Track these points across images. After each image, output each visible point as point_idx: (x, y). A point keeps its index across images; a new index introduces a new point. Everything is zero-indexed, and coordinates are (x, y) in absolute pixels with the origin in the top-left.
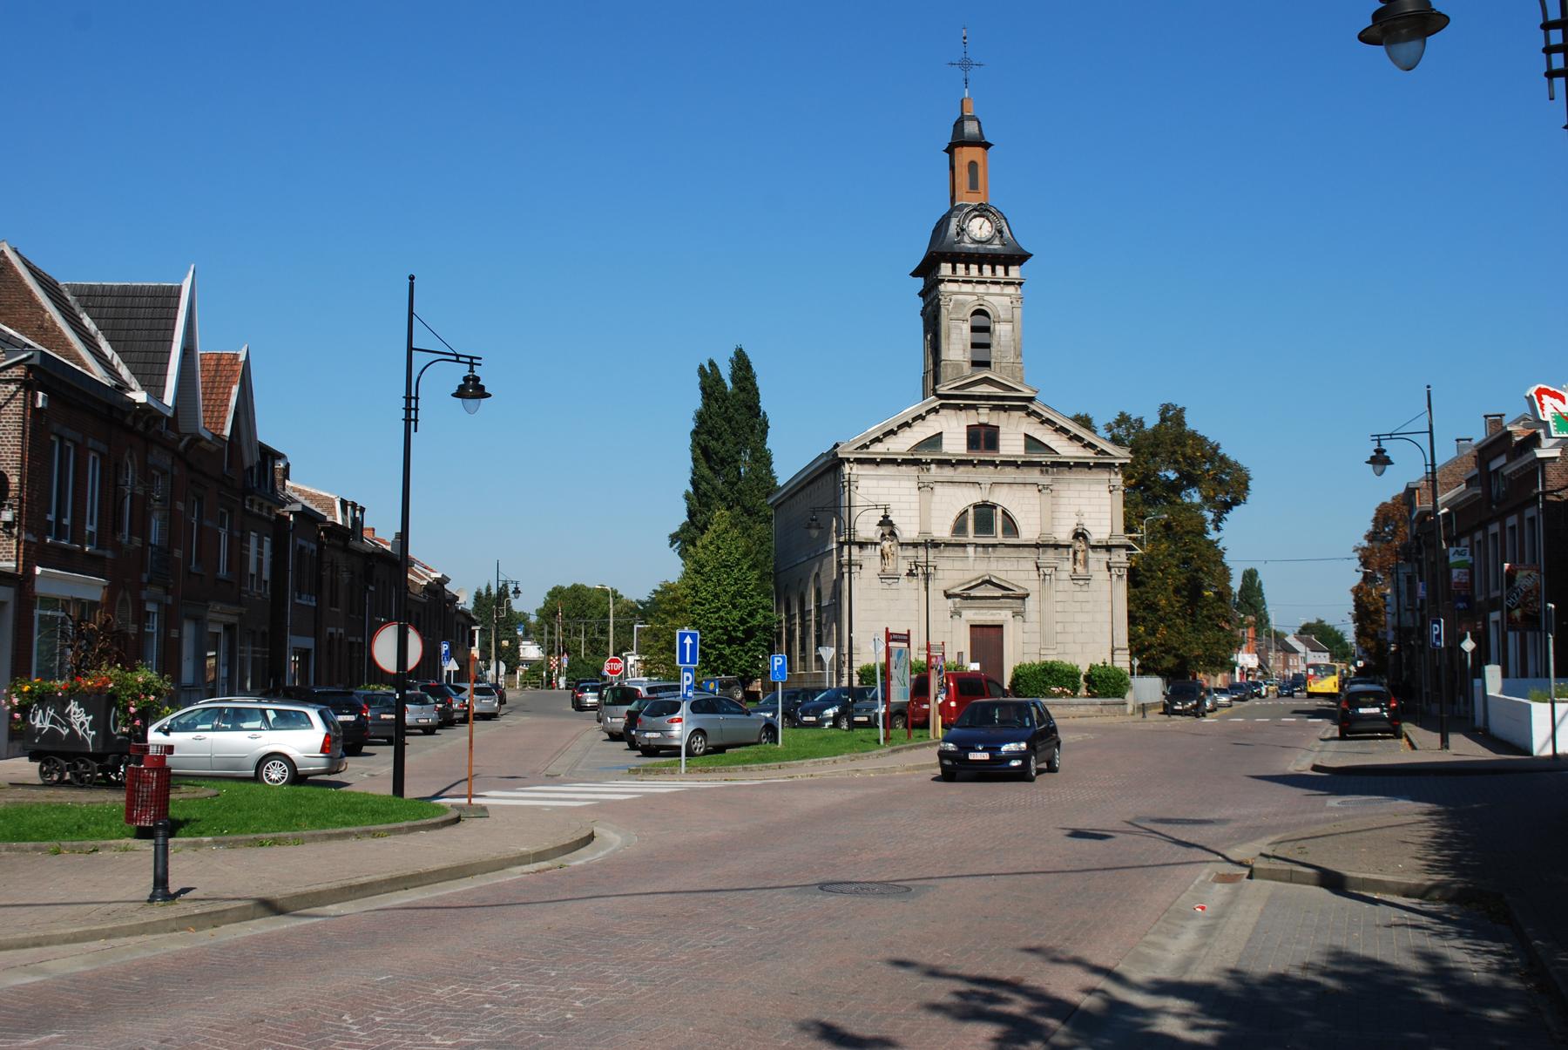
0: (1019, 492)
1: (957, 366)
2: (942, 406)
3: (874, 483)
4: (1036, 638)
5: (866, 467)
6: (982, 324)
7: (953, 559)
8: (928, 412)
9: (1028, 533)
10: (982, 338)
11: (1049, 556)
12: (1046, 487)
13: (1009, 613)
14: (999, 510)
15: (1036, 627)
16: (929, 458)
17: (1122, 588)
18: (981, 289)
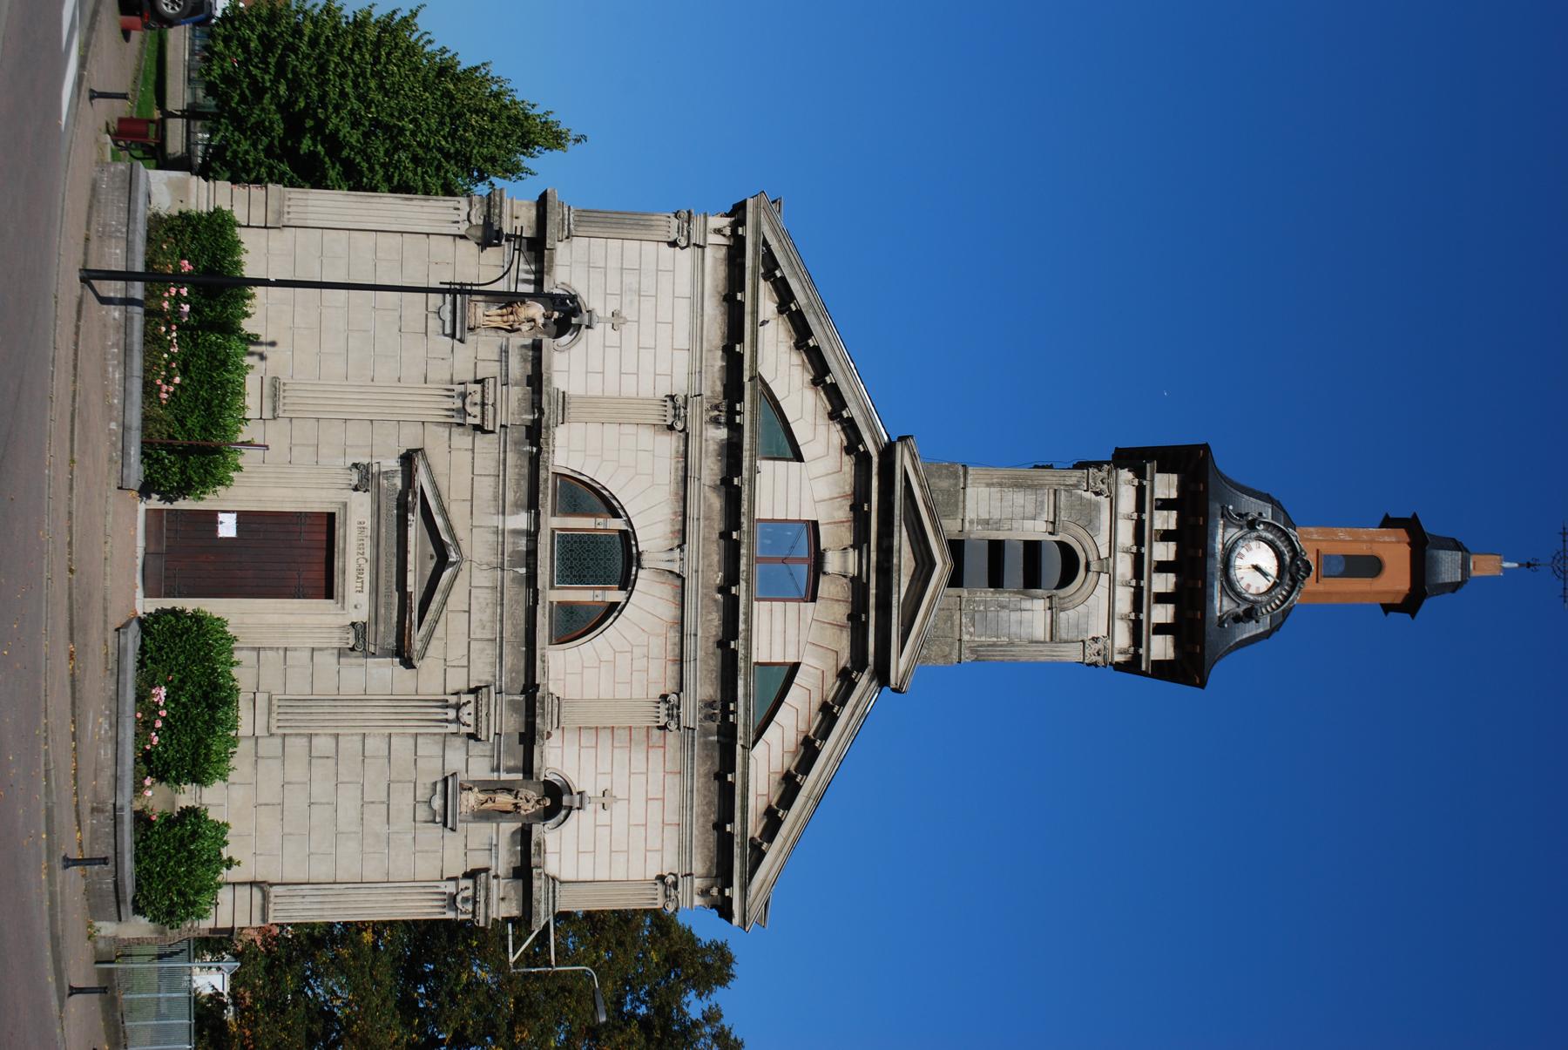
0: (661, 645)
1: (955, 501)
2: (862, 461)
3: (684, 286)
4: (298, 686)
5: (722, 271)
6: (1045, 567)
7: (500, 476)
8: (850, 427)
9: (567, 669)
10: (1014, 566)
11: (504, 720)
12: (674, 712)
13: (362, 615)
14: (616, 596)
15: (325, 686)
16: (746, 420)
17: (421, 907)
18: (1124, 566)
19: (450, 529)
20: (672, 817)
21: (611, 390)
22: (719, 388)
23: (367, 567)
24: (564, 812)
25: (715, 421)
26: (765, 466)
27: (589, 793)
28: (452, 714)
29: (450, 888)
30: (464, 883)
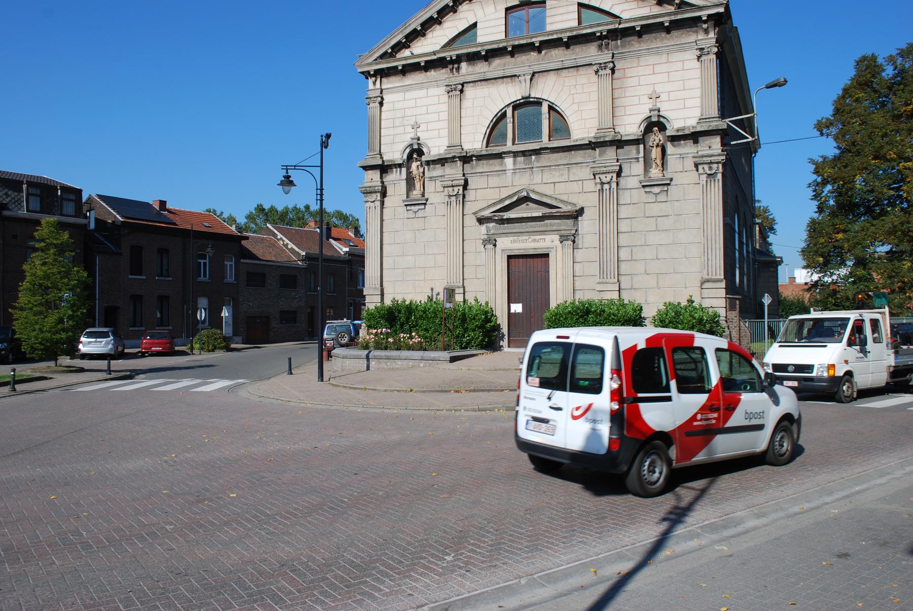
5: (392, 79)
7: (487, 174)
9: (582, 129)
12: (602, 66)
13: (556, 238)
15: (594, 255)
19: (510, 197)
20: (664, 58)
21: (445, 124)
22: (444, 71)
23: (533, 237)
24: (662, 120)
25: (458, 69)
26: (480, 40)
27: (650, 106)
28: (606, 187)
29: (704, 177)
30: (701, 171)
